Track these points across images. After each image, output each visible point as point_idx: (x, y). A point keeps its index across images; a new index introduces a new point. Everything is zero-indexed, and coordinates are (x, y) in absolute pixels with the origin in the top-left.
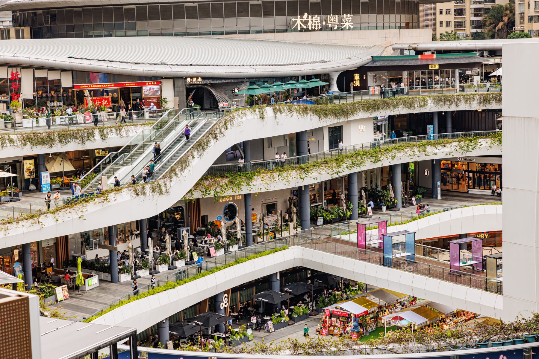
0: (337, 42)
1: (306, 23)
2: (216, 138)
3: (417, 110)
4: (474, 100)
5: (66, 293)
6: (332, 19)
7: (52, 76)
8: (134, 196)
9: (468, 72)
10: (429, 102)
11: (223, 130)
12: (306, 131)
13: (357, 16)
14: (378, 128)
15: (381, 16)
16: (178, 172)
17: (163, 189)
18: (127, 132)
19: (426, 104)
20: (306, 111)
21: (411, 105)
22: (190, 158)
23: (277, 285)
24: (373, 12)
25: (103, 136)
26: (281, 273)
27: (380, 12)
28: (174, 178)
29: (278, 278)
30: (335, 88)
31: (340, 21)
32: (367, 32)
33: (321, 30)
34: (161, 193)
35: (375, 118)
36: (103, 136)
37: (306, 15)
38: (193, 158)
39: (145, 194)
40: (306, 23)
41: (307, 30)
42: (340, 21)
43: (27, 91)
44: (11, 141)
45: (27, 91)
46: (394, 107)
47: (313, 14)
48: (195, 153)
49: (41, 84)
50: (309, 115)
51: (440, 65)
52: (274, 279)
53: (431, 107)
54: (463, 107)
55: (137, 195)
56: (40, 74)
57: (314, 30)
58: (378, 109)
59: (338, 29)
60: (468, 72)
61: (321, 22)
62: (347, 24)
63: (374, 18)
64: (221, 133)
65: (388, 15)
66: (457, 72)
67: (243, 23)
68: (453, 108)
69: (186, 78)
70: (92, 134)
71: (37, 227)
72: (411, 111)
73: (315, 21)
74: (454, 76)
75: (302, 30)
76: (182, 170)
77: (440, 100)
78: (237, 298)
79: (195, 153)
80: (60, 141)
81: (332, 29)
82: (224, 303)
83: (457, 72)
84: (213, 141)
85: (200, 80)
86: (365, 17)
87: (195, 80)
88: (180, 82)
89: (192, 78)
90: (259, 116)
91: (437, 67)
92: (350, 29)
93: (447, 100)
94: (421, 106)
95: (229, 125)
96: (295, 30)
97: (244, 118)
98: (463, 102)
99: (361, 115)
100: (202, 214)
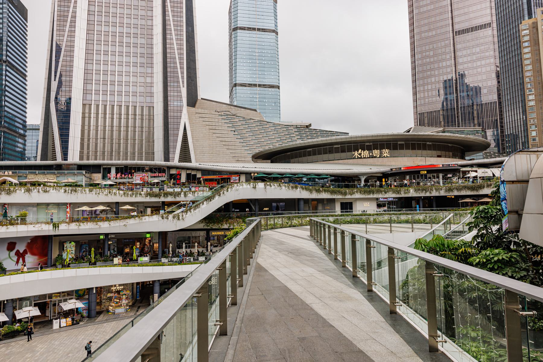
0: (379, 163)
1: (360, 154)
2: (220, 195)
3: (403, 195)
4: (441, 189)
5: (121, 262)
6: (376, 152)
7: (193, 173)
8: (161, 219)
9: (449, 176)
10: (411, 191)
11: (225, 192)
12: (303, 199)
14: (379, 206)
15: (414, 151)
17: (181, 218)
18: (198, 194)
19: (409, 192)
20: (296, 187)
21: (399, 192)
25: (185, 195)
27: (413, 148)
28: (189, 213)
30: (363, 183)
31: (381, 153)
33: (369, 158)
34: (179, 219)
35: (377, 199)
36: (185, 195)
37: (360, 150)
39: (168, 218)
40: (360, 154)
41: (361, 158)
42: (381, 153)
43: (183, 179)
44: (140, 194)
45: (183, 179)
46: (386, 193)
47: (364, 150)
48: (205, 203)
49: (188, 176)
50: (298, 189)
51: (427, 171)
53: (412, 193)
55: (163, 218)
56: (189, 172)
57: (365, 158)
58: (373, 193)
60: (449, 176)
61: (369, 154)
62: (385, 154)
63: (410, 152)
64: (223, 193)
65: (420, 151)
66: (441, 175)
67: (331, 156)
68: (428, 194)
69: (251, 173)
70: (180, 194)
71: (97, 227)
72: (398, 196)
73: (366, 153)
74: (438, 177)
75: (358, 158)
76: (195, 209)
77: (419, 190)
80: (164, 196)
81: (375, 157)
83: (441, 175)
88: (248, 176)
90: (252, 186)
91: (426, 172)
92: (387, 157)
93: (425, 190)
94: (405, 193)
95: (229, 190)
96: (354, 158)
97: (241, 187)
98: (434, 191)
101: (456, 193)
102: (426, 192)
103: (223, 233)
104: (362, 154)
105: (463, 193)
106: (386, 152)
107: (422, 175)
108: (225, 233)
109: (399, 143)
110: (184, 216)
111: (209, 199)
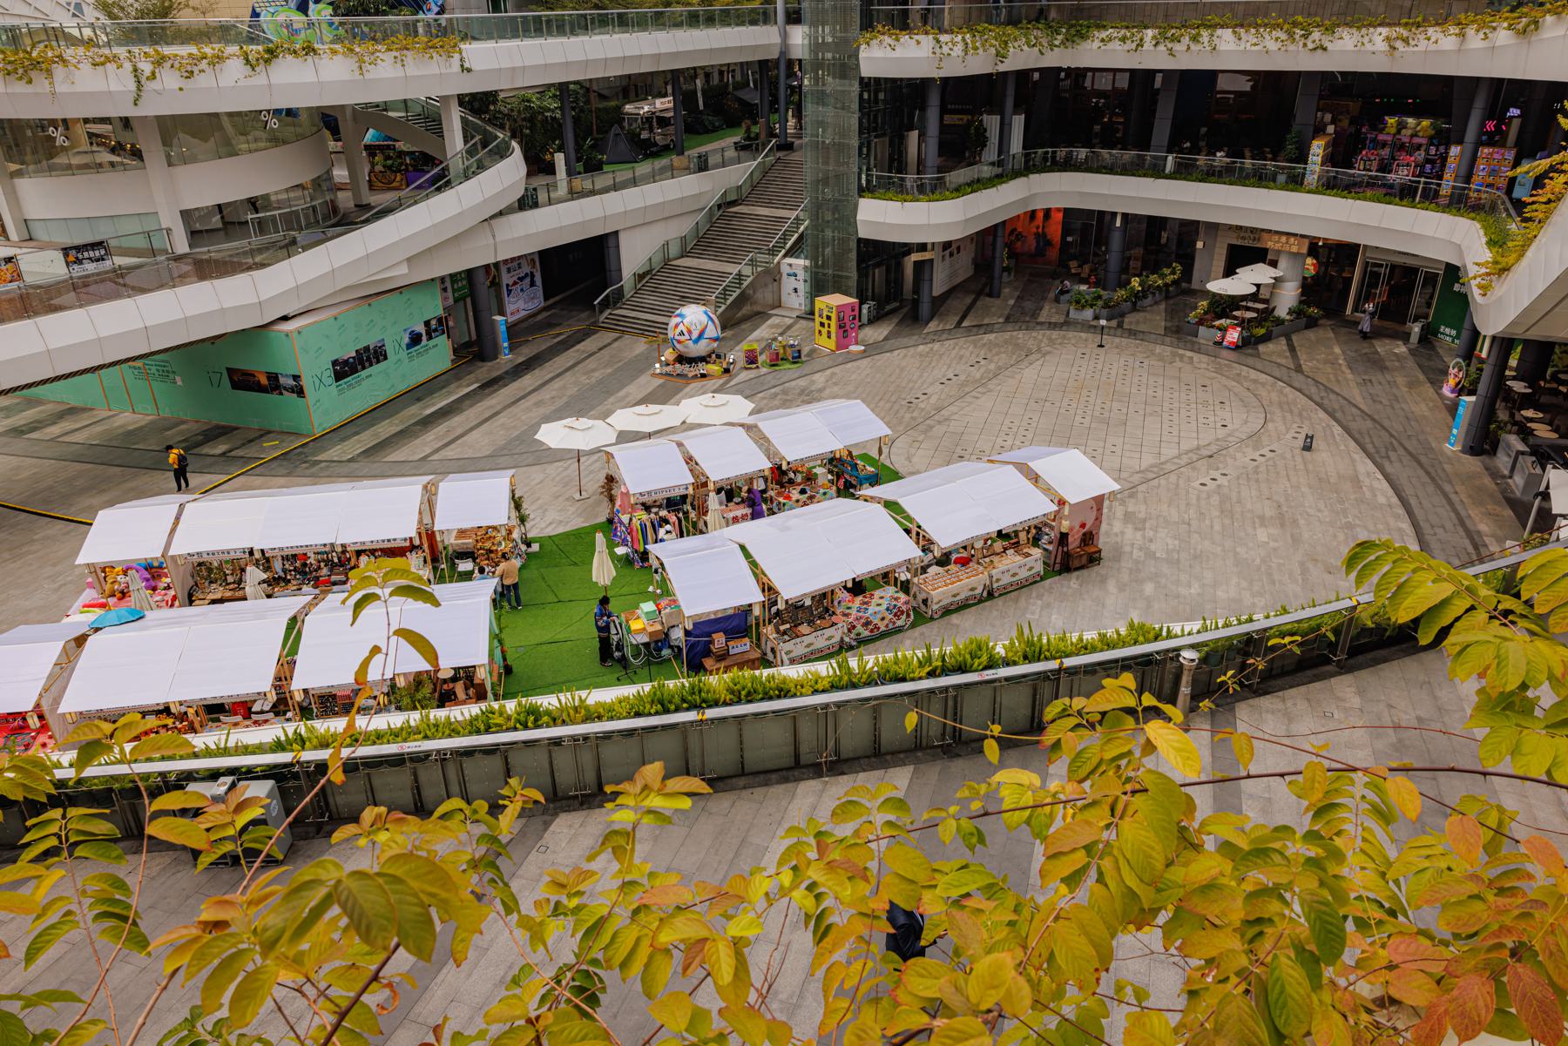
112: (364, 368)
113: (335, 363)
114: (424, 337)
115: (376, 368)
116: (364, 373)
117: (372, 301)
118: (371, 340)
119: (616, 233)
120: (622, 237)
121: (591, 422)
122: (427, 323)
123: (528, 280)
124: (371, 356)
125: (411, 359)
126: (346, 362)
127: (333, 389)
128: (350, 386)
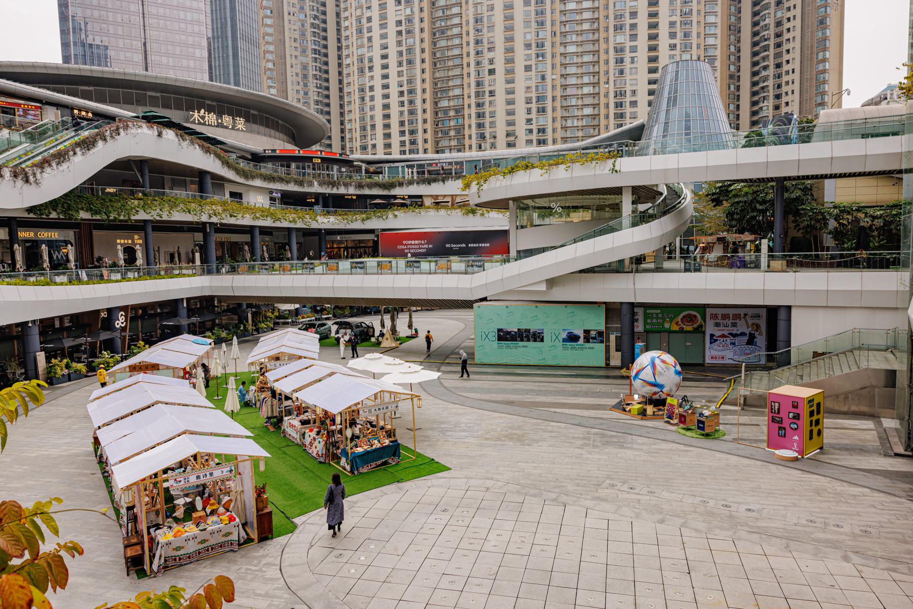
2: (105, 140)
6: (227, 119)
10: (316, 183)
13: (248, 124)
16: (54, 164)
17: (31, 179)
22: (71, 153)
23: (183, 312)
24: (261, 124)
26: (188, 300)
27: (267, 126)
28: (48, 170)
29: (185, 305)
31: (234, 123)
32: (258, 137)
34: (27, 181)
37: (202, 111)
38: (75, 154)
40: (203, 118)
41: (204, 124)
42: (234, 123)
47: (209, 113)
48: (78, 150)
52: (180, 307)
54: (342, 190)
59: (233, 128)
63: (262, 129)
68: (335, 191)
69: (72, 109)
78: (138, 328)
79: (78, 150)
81: (226, 127)
82: (120, 322)
84: (100, 143)
85: (90, 115)
86: (255, 126)
87: (84, 113)
89: (80, 110)
92: (242, 130)
99: (258, 183)
100: (96, 255)
101: (367, 192)
102: (333, 186)
103: (32, 234)
104: (207, 118)
105: (375, 192)
106: (241, 123)
107: (314, 164)
108: (36, 235)
109: (252, 112)
110: (38, 176)
111: (87, 145)
112: (522, 340)
113: (499, 330)
114: (582, 340)
115: (531, 344)
116: (521, 344)
117: (538, 305)
118: (534, 327)
119: (789, 308)
120: (794, 311)
121: (402, 362)
122: (587, 332)
123: (746, 338)
124: (523, 335)
125: (565, 348)
126: (509, 333)
127: (496, 344)
128: (508, 347)
